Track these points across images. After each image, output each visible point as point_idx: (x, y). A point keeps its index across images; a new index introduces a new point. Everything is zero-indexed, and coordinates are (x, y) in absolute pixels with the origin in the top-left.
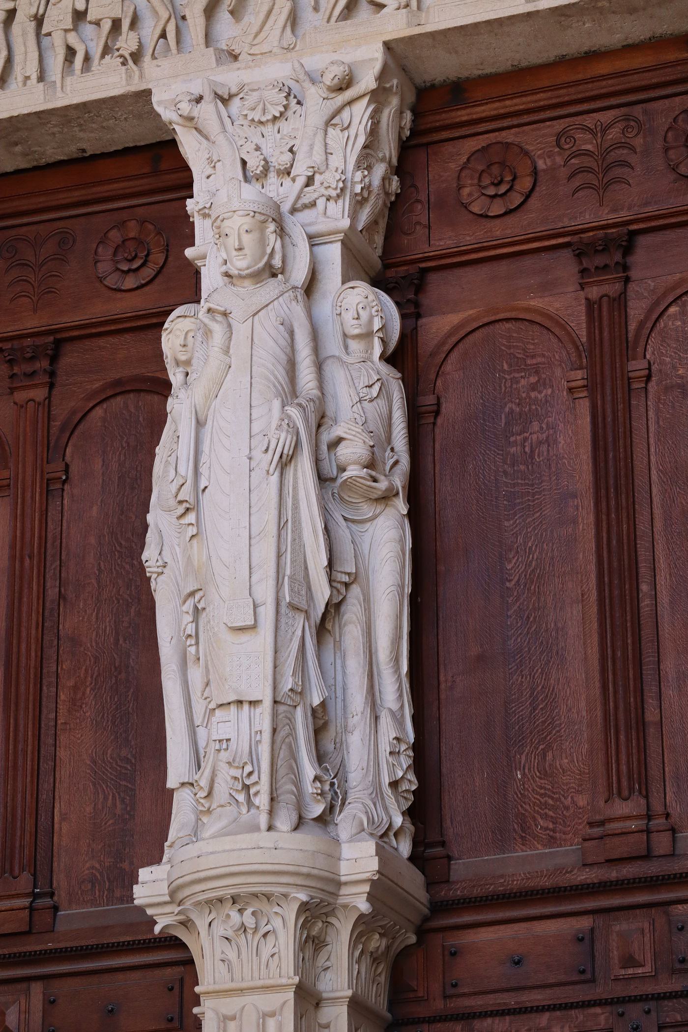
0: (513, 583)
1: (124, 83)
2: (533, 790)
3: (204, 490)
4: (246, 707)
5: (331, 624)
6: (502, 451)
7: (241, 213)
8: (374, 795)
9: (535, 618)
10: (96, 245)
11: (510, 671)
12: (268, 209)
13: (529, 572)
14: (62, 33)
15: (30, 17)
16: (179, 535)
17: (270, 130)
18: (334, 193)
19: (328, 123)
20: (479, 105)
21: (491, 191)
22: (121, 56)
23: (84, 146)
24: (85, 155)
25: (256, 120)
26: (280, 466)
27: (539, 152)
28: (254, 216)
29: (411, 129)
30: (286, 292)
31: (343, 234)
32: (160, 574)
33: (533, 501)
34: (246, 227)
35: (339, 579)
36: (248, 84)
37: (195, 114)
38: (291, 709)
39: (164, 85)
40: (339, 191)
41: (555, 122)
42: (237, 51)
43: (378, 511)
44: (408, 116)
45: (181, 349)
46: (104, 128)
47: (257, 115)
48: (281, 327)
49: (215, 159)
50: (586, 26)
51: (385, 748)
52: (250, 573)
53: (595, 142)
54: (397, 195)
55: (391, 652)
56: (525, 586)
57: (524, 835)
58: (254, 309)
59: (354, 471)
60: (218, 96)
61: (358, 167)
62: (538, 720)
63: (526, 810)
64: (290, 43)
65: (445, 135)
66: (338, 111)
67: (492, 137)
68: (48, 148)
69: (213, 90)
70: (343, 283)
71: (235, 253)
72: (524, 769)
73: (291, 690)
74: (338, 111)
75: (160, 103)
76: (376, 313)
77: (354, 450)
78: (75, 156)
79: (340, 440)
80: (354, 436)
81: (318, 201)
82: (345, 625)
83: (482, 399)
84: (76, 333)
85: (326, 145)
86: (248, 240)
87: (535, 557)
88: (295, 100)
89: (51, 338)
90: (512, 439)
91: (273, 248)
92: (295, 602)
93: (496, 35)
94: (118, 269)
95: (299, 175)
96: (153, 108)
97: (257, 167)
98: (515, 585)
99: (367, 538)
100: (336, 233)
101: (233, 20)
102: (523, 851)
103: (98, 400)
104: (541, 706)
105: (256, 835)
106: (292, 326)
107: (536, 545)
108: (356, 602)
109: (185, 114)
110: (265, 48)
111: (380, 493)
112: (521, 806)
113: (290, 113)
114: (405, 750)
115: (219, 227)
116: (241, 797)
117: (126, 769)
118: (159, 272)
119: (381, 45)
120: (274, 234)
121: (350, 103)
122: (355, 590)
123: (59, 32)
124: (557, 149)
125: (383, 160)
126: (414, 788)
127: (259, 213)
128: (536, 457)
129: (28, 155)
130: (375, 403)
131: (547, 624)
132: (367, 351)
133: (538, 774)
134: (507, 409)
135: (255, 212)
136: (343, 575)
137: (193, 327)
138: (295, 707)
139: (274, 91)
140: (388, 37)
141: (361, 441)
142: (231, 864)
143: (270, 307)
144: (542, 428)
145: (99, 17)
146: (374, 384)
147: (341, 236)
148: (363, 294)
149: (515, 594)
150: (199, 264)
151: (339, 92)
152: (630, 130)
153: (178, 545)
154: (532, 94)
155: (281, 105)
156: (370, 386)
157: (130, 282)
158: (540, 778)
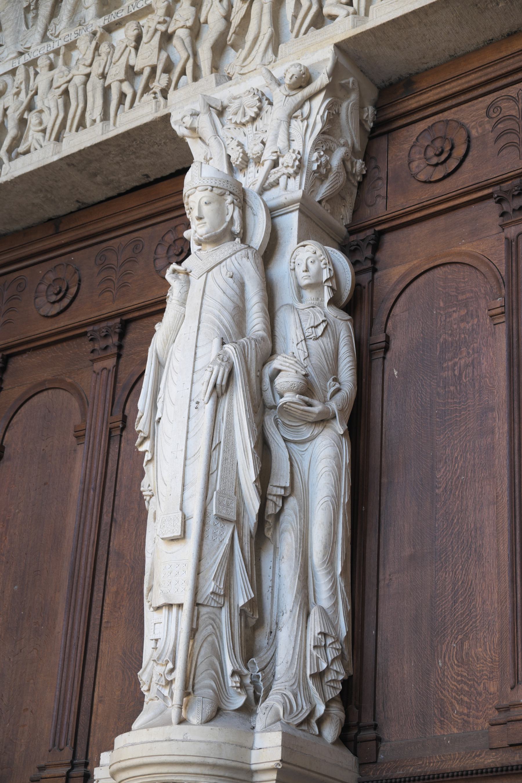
0: (441, 490)
1: (154, 111)
2: (452, 677)
3: (159, 422)
5: (270, 533)
8: (295, 687)
9: (458, 519)
12: (237, 190)
14: (118, 83)
15: (99, 76)
17: (250, 129)
18: (291, 171)
19: (291, 117)
20: (425, 93)
21: (435, 161)
23: (147, 171)
25: (238, 122)
26: (214, 395)
27: (473, 124)
29: (374, 122)
30: (238, 251)
31: (299, 204)
33: (460, 416)
34: (205, 200)
35: (274, 493)
37: (196, 125)
38: (215, 610)
43: (316, 432)
46: (152, 153)
48: (230, 279)
51: (310, 643)
52: (183, 490)
53: (517, 107)
54: (364, 176)
55: (324, 556)
56: (451, 492)
57: (442, 719)
58: (209, 266)
59: (289, 397)
62: (458, 612)
63: (445, 696)
66: (300, 106)
67: (436, 118)
68: (120, 176)
69: (208, 104)
70: (298, 243)
72: (445, 657)
73: (213, 593)
74: (300, 106)
76: (324, 266)
77: (287, 380)
80: (288, 367)
84: (136, 314)
87: (460, 465)
88: (267, 102)
89: (118, 320)
90: (445, 365)
91: (232, 217)
92: (224, 514)
96: (172, 128)
97: (238, 159)
98: (443, 491)
99: (307, 456)
104: (460, 600)
105: (168, 728)
106: (242, 278)
107: (461, 455)
108: (292, 512)
109: (188, 126)
110: (251, 67)
111: (315, 416)
112: (441, 692)
113: (263, 114)
114: (332, 643)
119: (332, 47)
120: (232, 205)
121: (310, 98)
125: (345, 145)
126: (341, 678)
127: (217, 187)
128: (463, 378)
129: (109, 184)
130: (320, 341)
131: (467, 524)
132: (318, 299)
134: (441, 340)
135: (213, 187)
136: (279, 489)
138: (221, 608)
139: (249, 96)
141: (293, 371)
142: (144, 755)
143: (224, 263)
144: (468, 353)
145: (142, 67)
146: (320, 324)
147: (297, 206)
148: (312, 250)
149: (443, 499)
151: (299, 90)
154: (466, 76)
155: (255, 107)
156: (316, 327)
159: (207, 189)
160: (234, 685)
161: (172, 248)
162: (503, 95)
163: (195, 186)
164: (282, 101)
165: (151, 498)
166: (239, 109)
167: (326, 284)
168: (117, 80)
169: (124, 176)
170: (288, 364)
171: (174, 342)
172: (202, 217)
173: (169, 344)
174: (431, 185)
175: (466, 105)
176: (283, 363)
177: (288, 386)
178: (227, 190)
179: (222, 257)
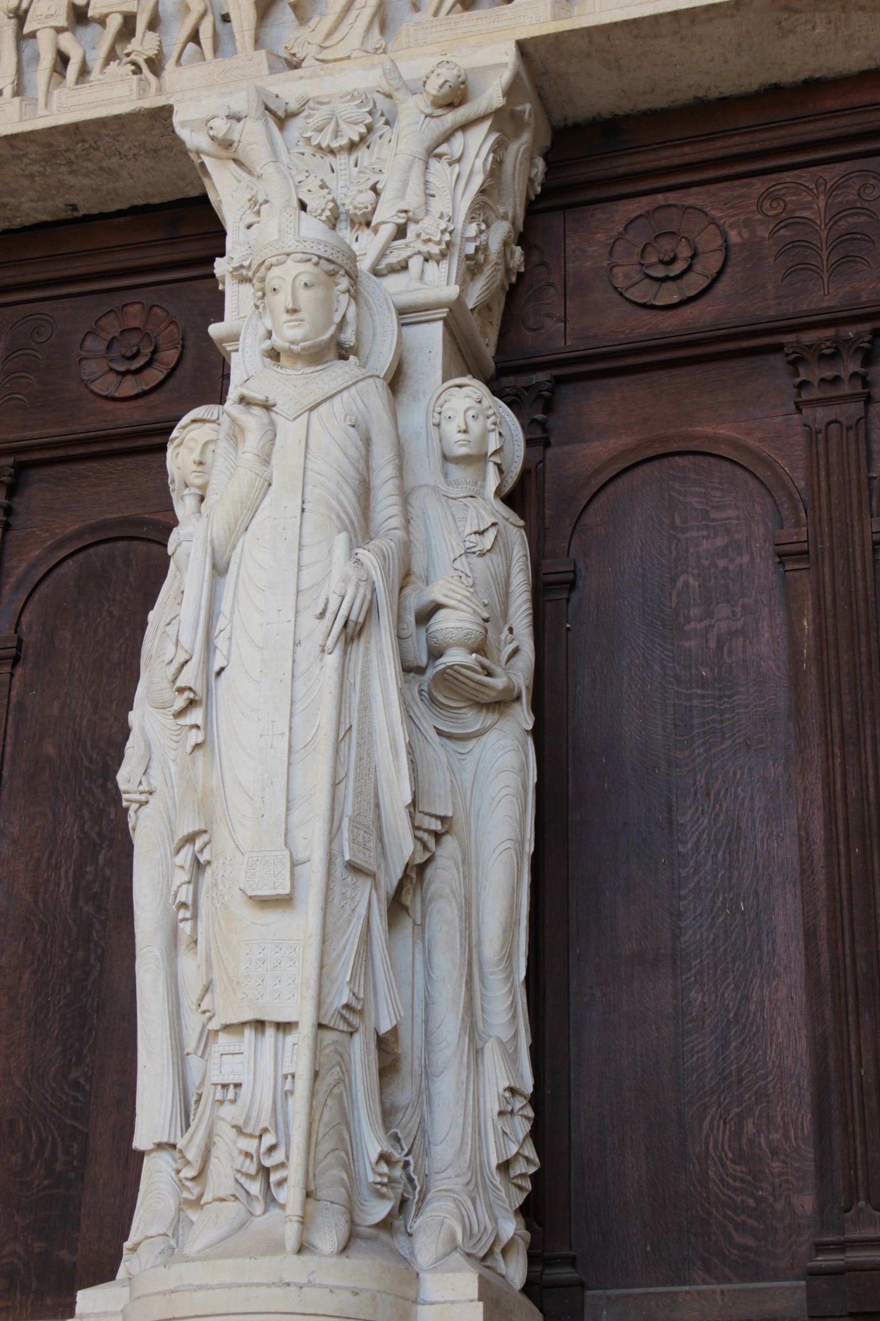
0: (689, 846)
1: (134, 97)
3: (219, 673)
4: (270, 1032)
5: (410, 897)
6: (672, 645)
7: (299, 256)
8: (471, 1186)
10: (82, 336)
11: (683, 985)
13: (714, 830)
14: (52, 32)
15: (10, 12)
16: (175, 745)
17: (343, 161)
18: (435, 250)
19: (432, 153)
22: (134, 63)
24: (76, 214)
25: (324, 145)
26: (343, 638)
27: (731, 220)
28: (317, 264)
29: (542, 185)
32: (142, 804)
33: (721, 722)
34: (304, 279)
35: (426, 826)
37: (235, 136)
38: (344, 1038)
39: (191, 99)
40: (443, 246)
41: (755, 180)
42: (300, 56)
43: (489, 722)
44: (540, 163)
45: (195, 467)
46: (102, 169)
47: (325, 139)
48: (352, 430)
49: (261, 199)
50: (817, 31)
51: (492, 1105)
52: (288, 809)
54: (520, 275)
55: (503, 946)
56: (708, 852)
57: (706, 1255)
58: (312, 399)
59: (455, 657)
61: (471, 217)
64: (378, 46)
66: (447, 137)
68: (23, 199)
69: (264, 102)
70: (444, 380)
71: (286, 317)
73: (347, 1006)
74: (447, 137)
75: (183, 124)
76: (493, 427)
78: (62, 216)
79: (437, 607)
80: (460, 601)
81: (411, 263)
82: (432, 899)
83: (642, 568)
84: (46, 455)
85: (426, 182)
87: (724, 806)
88: (383, 120)
89: (10, 460)
91: (344, 317)
92: (360, 860)
93: (682, 39)
95: (384, 223)
97: (323, 211)
98: (692, 848)
100: (437, 308)
101: (296, 23)
102: (705, 1282)
106: (368, 431)
107: (727, 790)
109: (220, 135)
111: (493, 694)
113: (374, 138)
114: (522, 1108)
115: (263, 280)
116: (255, 1188)
117: (76, 1100)
118: (169, 376)
120: (347, 295)
121: (464, 127)
122: (450, 844)
123: (48, 31)
124: (759, 217)
125: (504, 217)
126: (532, 1170)
127: (328, 260)
128: (725, 656)
132: (476, 483)
133: (730, 1155)
134: (679, 584)
135: (320, 257)
136: (433, 820)
138: (351, 1034)
140: (525, 33)
141: (469, 610)
142: (232, 1311)
144: (734, 613)
145: (105, 11)
146: (487, 529)
147: (443, 313)
148: (475, 396)
149: (692, 863)
150: (228, 349)
152: (867, 191)
153: (174, 761)
156: (481, 533)
158: (734, 1162)
159: (309, 260)
160: (378, 1179)
161: (116, 345)
162: (788, 180)
163: (288, 250)
164: (417, 122)
165: (141, 806)
166: (329, 123)
167: (492, 459)
168: (51, 27)
169: (32, 201)
170: (459, 597)
171: (246, 530)
172: (297, 308)
173: (237, 534)
174: (654, 312)
175: (719, 186)
176: (451, 594)
177: (460, 636)
178: (341, 266)
179: (333, 387)
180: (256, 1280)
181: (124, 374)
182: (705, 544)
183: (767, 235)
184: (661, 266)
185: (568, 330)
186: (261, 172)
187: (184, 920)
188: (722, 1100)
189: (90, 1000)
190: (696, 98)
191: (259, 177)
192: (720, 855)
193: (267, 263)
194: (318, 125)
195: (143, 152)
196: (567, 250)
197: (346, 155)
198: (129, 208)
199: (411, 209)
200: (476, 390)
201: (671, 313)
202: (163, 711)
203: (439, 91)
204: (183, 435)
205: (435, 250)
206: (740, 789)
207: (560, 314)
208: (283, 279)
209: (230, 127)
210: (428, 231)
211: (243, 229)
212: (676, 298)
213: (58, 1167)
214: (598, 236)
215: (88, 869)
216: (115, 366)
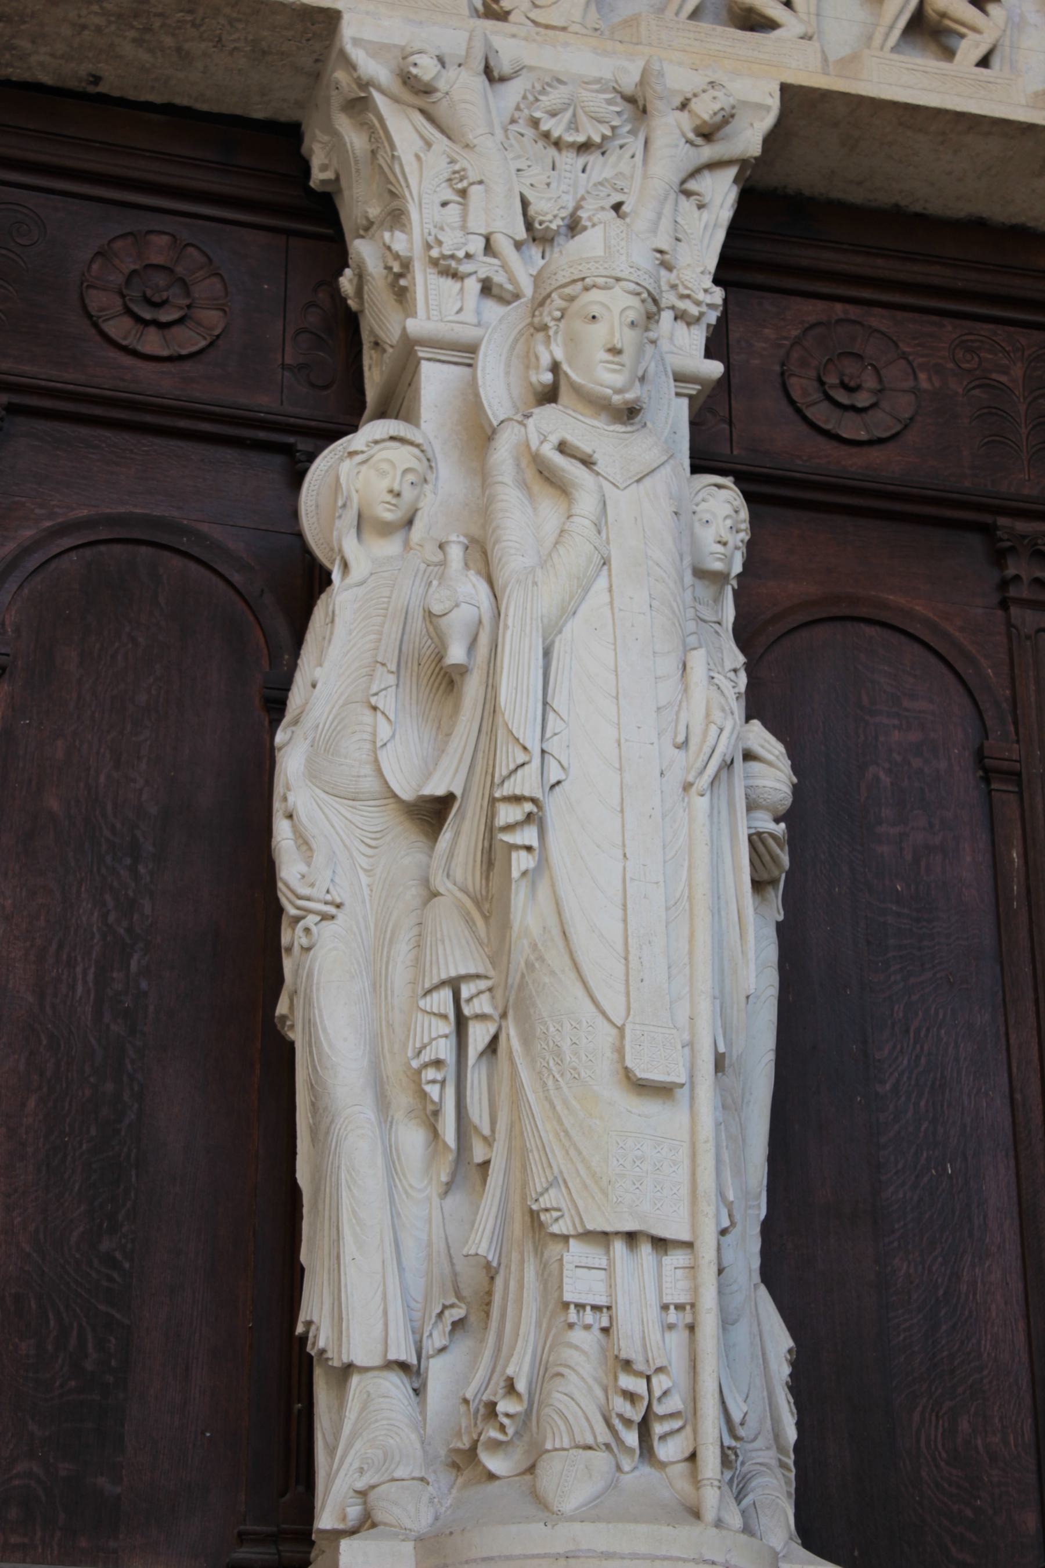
0: (888, 1087)
3: (553, 787)
4: (646, 1249)
16: (369, 851)
24: (91, 89)
25: (555, 134)
27: (921, 360)
31: (699, 387)
32: (326, 917)
34: (631, 315)
36: (531, 69)
37: (442, 85)
39: (367, 13)
45: (389, 498)
46: (179, 50)
47: (557, 127)
49: (473, 175)
60: (488, 71)
64: (597, 26)
65: (760, 278)
66: (696, 173)
67: (854, 312)
74: (696, 173)
75: (356, 42)
77: (778, 785)
78: (72, 84)
86: (626, 338)
87: (926, 1047)
94: (129, 312)
97: (555, 216)
103: (80, 542)
107: (928, 1030)
115: (572, 299)
116: (631, 1438)
117: (110, 1279)
118: (211, 344)
124: (951, 365)
133: (944, 1455)
135: (650, 294)
137: (414, 463)
140: (791, 79)
147: (693, 389)
148: (736, 503)
157: (152, 343)
159: (638, 294)
163: (620, 275)
165: (321, 920)
166: (565, 110)
169: (52, 55)
171: (574, 613)
174: (835, 444)
175: (906, 314)
180: (675, 1553)
181: (146, 323)
182: (896, 735)
183: (960, 391)
184: (842, 391)
185: (735, 437)
186: (475, 142)
187: (434, 1082)
188: (933, 1389)
189: (125, 1150)
190: (897, 205)
191: (467, 146)
192: (923, 1103)
193: (588, 281)
194: (554, 107)
195: (248, 49)
196: (731, 337)
197: (575, 155)
198: (163, 105)
199: (670, 252)
200: (737, 497)
201: (854, 450)
202: (351, 803)
203: (711, 118)
204: (372, 452)
205: (694, 310)
206: (943, 1032)
207: (724, 412)
208: (608, 308)
209: (439, 72)
210: (690, 285)
211: (437, 207)
212: (863, 435)
213: (89, 1366)
214: (767, 331)
215: (115, 975)
216: (136, 309)
